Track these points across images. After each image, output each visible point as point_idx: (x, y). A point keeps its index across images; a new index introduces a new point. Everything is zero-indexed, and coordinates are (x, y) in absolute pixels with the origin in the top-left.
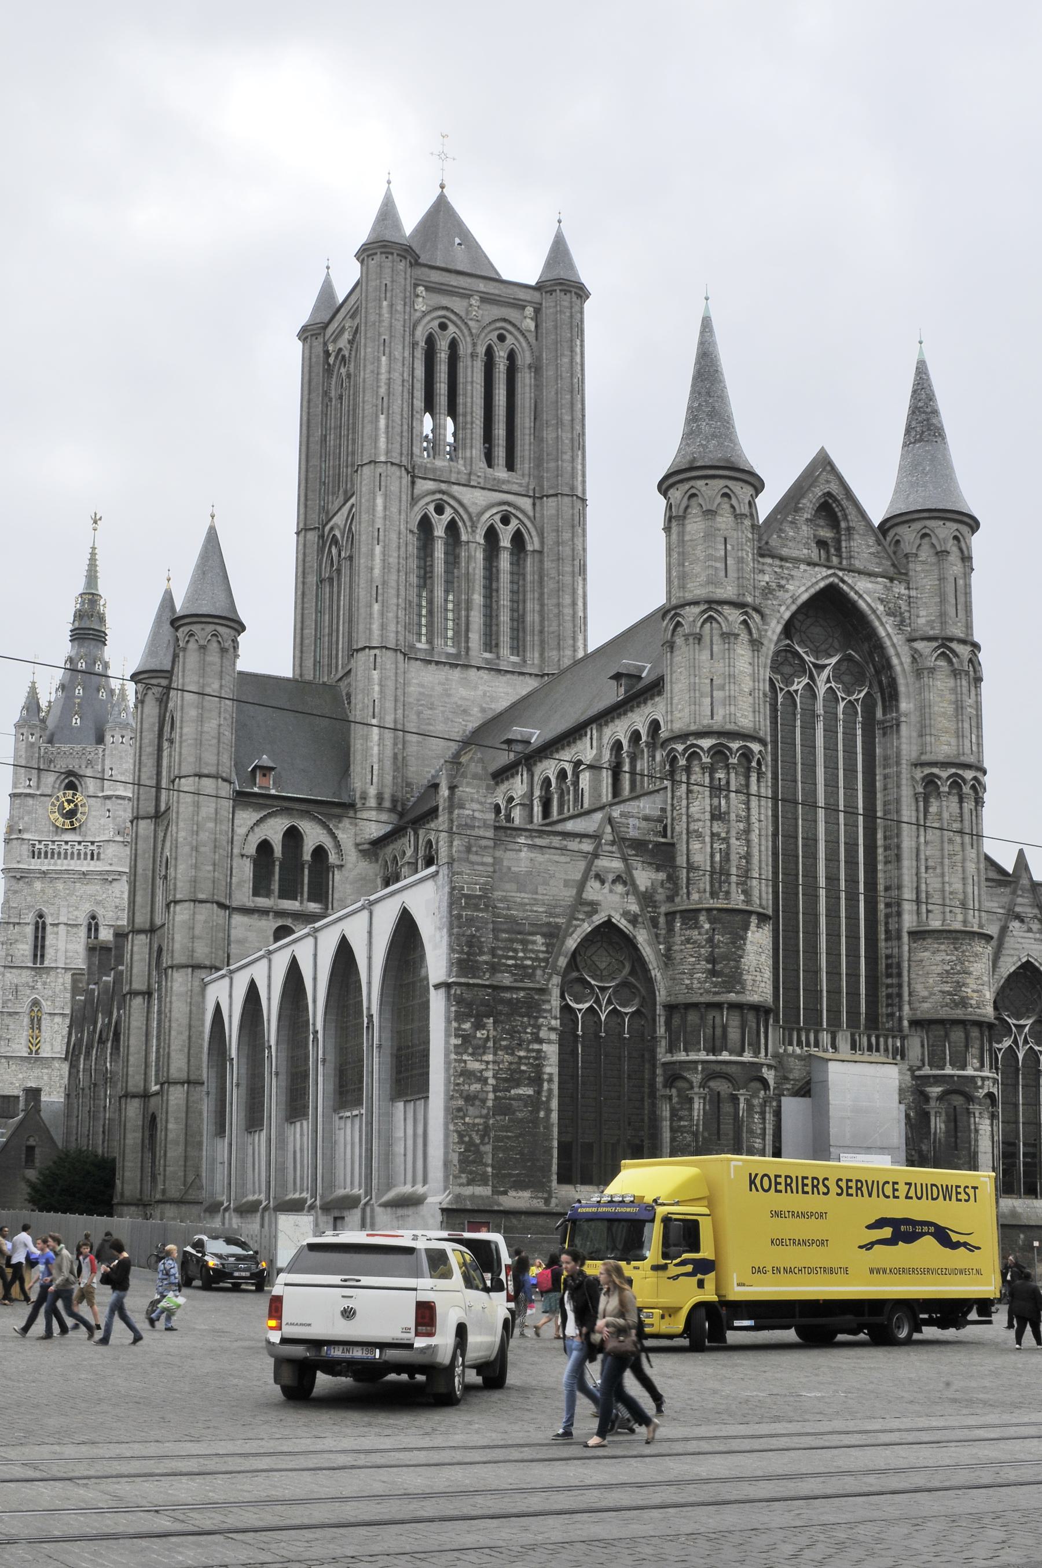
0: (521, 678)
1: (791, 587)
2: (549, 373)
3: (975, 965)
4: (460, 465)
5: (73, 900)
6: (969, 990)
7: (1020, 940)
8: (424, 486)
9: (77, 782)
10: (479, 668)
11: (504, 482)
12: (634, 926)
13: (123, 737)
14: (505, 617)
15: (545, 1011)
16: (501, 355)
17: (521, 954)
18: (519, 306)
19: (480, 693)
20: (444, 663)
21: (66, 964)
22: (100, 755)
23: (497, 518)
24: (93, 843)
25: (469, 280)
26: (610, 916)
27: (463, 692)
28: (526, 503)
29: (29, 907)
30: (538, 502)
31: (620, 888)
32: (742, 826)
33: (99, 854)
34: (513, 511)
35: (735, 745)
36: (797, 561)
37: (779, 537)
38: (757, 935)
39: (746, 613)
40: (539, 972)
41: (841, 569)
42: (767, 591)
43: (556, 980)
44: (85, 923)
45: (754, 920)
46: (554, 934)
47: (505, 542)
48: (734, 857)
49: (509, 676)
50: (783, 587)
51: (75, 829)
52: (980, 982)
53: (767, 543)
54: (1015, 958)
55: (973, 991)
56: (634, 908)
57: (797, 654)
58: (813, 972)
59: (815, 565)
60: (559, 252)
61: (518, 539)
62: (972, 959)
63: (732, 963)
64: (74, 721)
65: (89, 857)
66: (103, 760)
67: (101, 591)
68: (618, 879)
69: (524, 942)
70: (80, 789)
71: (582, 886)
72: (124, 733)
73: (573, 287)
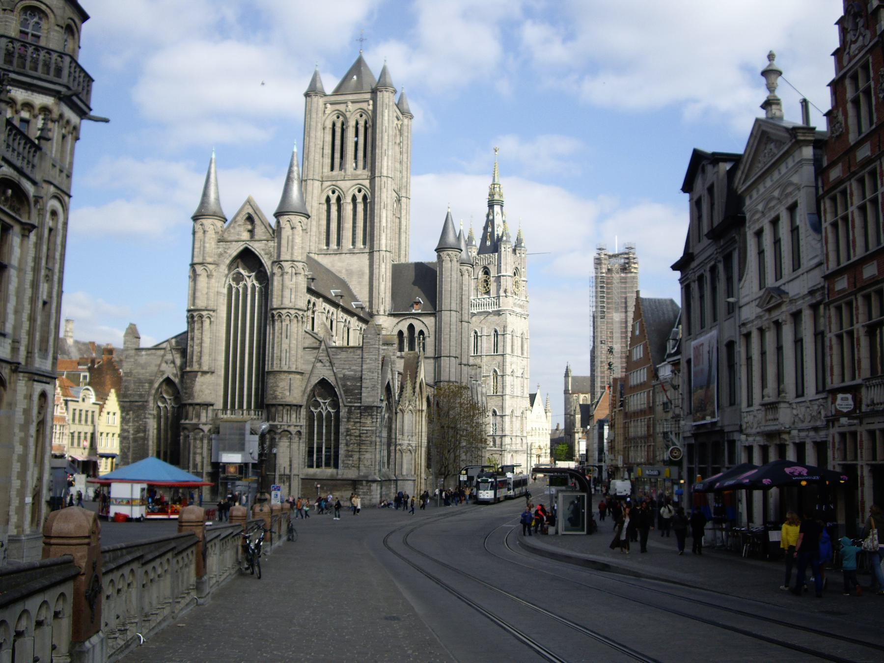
1: (229, 251)
4: (342, 172)
11: (360, 175)
16: (362, 123)
27: (339, 264)
28: (367, 183)
32: (199, 341)
35: (195, 314)
42: (220, 255)
43: (151, 398)
44: (493, 333)
45: (199, 374)
46: (151, 383)
47: (360, 199)
48: (195, 353)
56: (175, 372)
57: (241, 274)
60: (384, 72)
69: (143, 386)
71: (160, 366)
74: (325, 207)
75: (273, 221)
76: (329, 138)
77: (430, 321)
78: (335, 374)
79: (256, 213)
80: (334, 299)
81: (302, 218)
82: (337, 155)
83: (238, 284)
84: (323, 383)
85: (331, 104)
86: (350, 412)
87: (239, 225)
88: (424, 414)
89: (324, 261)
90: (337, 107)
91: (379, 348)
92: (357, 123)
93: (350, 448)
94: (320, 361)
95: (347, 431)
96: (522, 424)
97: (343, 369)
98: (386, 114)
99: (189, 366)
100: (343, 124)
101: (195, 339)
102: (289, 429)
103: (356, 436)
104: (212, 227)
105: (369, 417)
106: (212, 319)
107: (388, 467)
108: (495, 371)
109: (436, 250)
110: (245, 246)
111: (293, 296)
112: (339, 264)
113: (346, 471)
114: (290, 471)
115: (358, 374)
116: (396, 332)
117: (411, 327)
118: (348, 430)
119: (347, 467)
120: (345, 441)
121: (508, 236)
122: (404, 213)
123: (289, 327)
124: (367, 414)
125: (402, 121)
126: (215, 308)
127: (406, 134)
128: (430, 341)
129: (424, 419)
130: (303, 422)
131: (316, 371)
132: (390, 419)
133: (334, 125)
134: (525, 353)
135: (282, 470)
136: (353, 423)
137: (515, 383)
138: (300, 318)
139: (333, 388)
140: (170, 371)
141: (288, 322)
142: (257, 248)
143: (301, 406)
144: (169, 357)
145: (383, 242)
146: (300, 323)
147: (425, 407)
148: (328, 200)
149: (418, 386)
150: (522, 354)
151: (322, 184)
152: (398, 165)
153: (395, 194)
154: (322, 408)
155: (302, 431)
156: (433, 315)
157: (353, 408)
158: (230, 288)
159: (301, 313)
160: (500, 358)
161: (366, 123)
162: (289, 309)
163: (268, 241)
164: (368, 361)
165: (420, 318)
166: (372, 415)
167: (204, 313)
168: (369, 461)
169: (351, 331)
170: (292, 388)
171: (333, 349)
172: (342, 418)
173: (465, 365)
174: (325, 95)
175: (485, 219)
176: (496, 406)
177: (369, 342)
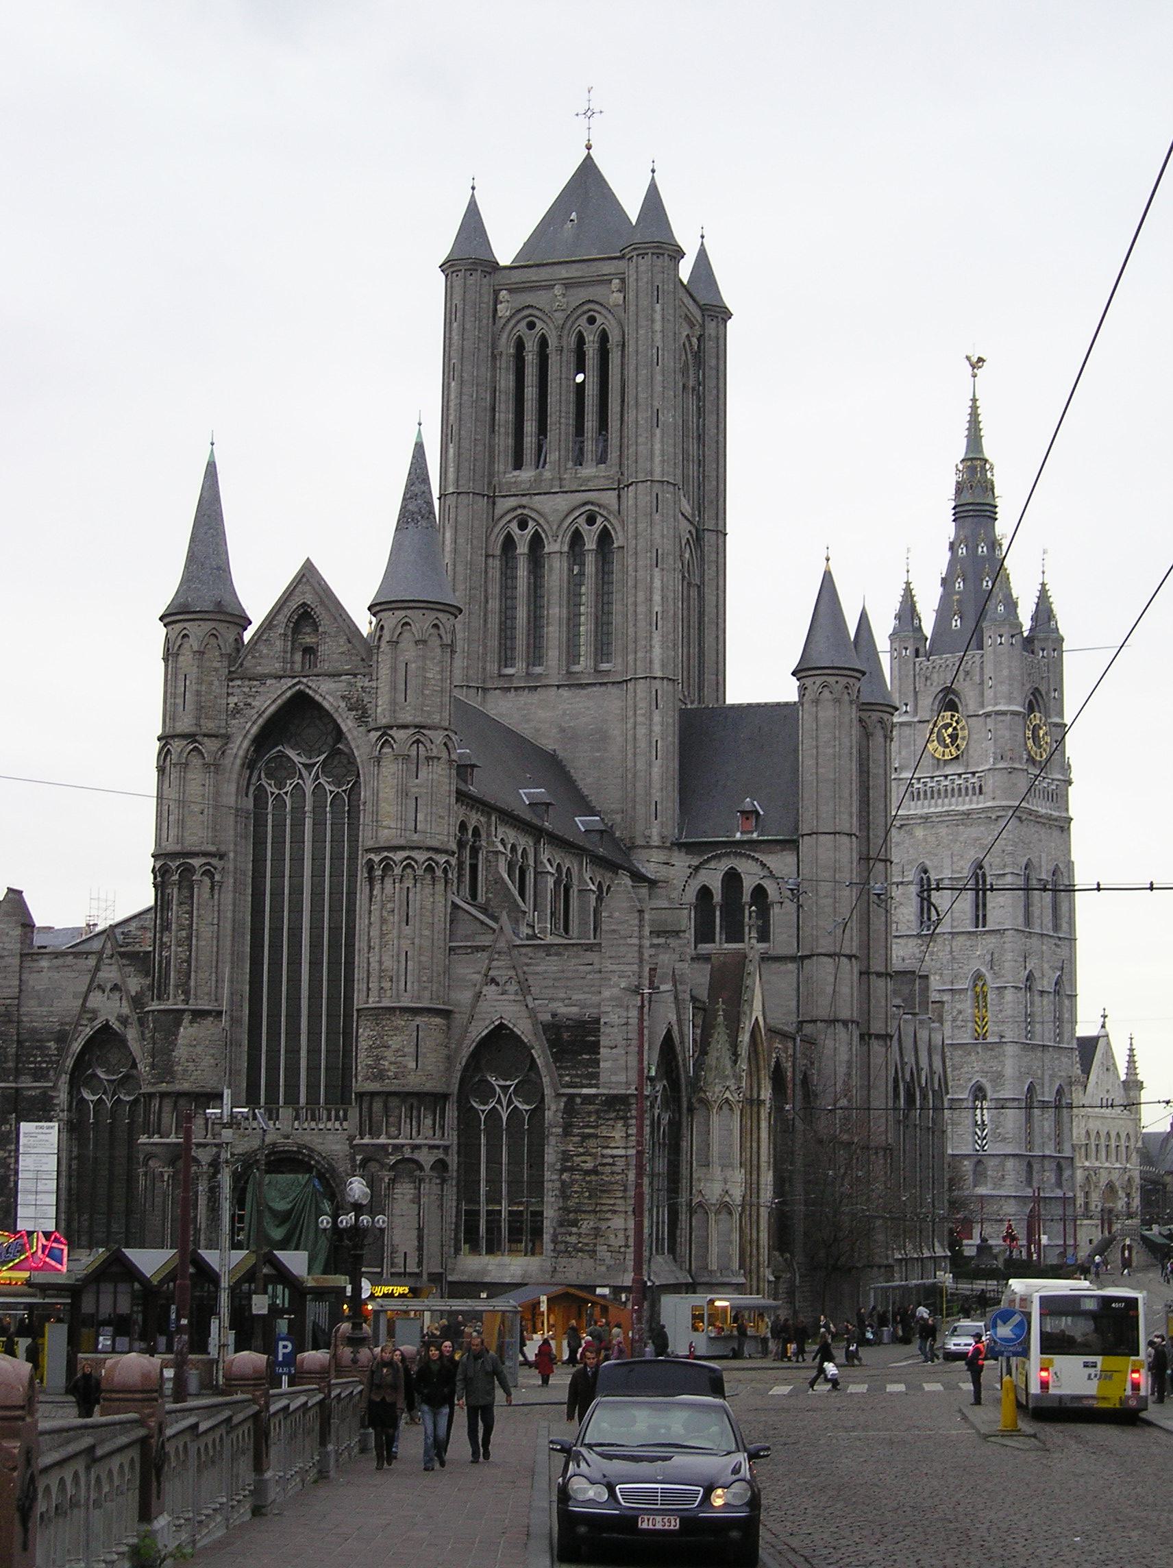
0: (603, 688)
2: (631, 348)
3: (395, 1038)
5: (956, 847)
6: (386, 1063)
7: (495, 1004)
8: (504, 504)
9: (956, 700)
10: (558, 687)
11: (588, 480)
12: (126, 1027)
13: (1001, 636)
14: (586, 627)
15: (56, 1105)
16: (591, 340)
17: (39, 1059)
18: (605, 281)
19: (561, 712)
20: (523, 688)
21: (952, 927)
22: (978, 663)
23: (582, 520)
24: (974, 773)
25: (548, 269)
26: (107, 1021)
27: (542, 714)
28: (610, 498)
29: (910, 862)
30: (624, 493)
31: (117, 995)
32: (184, 933)
33: (980, 787)
34: (597, 509)
35: (173, 865)
36: (262, 678)
37: (253, 657)
38: (190, 1030)
39: (196, 741)
40: (52, 1073)
41: (304, 677)
42: (236, 712)
43: (65, 1078)
45: (187, 1018)
46: (63, 1038)
47: (590, 544)
49: (590, 689)
50: (250, 705)
51: (957, 758)
52: (400, 1054)
53: (241, 665)
54: (487, 1022)
55: (391, 1063)
56: (126, 1010)
57: (288, 757)
58: (293, 1051)
59: (281, 677)
60: (653, 201)
61: (605, 537)
62: (390, 1033)
63: (165, 1057)
64: (954, 623)
65: (970, 792)
66: (982, 669)
67: (987, 454)
68: (115, 988)
70: (960, 709)
72: (1002, 631)
73: (648, 248)
74: (496, 563)
75: (364, 623)
76: (506, 381)
77: (781, 863)
78: (532, 1014)
79: (322, 602)
80: (528, 816)
81: (440, 615)
82: (530, 427)
83: (281, 785)
84: (500, 1036)
85: (510, 291)
86: (570, 1109)
87: (285, 635)
88: (764, 1114)
89: (502, 708)
90: (528, 298)
91: (641, 946)
92: (581, 340)
93: (570, 1203)
94: (493, 981)
95: (565, 1160)
96: (1058, 1123)
97: (552, 999)
98: (658, 317)
99: (159, 998)
100: (543, 342)
101: (174, 927)
102: (416, 1156)
103: (587, 1173)
104: (213, 641)
105: (620, 1124)
106: (217, 878)
107: (672, 1250)
108: (978, 976)
109: (794, 674)
110: (297, 687)
111: (420, 817)
112: (542, 714)
113: (563, 1261)
114: (420, 1264)
115: (590, 1012)
116: (691, 896)
117: (732, 879)
118: (566, 1156)
119: (564, 1251)
120: (558, 1184)
121: (1012, 605)
122: (710, 573)
123: (411, 895)
124: (613, 1115)
125: (703, 326)
126: (223, 849)
127: (713, 362)
128: (781, 916)
129: (764, 1124)
130: (452, 1139)
131: (483, 1006)
132: (675, 1126)
133: (520, 345)
134: (1065, 926)
135: (399, 1260)
136: (577, 1139)
137: (1037, 1009)
138: (439, 873)
139: (526, 1049)
140: (109, 1008)
141: (409, 883)
142: (327, 693)
143: (445, 1097)
144: (109, 974)
145: (657, 651)
146: (440, 887)
147: (766, 1094)
148: (509, 543)
149: (745, 1038)
150: (1056, 927)
151: (494, 503)
152: (693, 448)
153: (684, 523)
154: (499, 1102)
155: (448, 1159)
156: (791, 844)
157: (578, 1100)
158: (260, 797)
159: (442, 859)
160: (992, 940)
161: (604, 338)
162: (412, 848)
163: (355, 675)
164: (615, 979)
165: (757, 856)
166: (625, 1118)
167: (196, 862)
168: (621, 1235)
169: (574, 892)
170: (422, 1050)
171: (523, 950)
172: (551, 1126)
173: (879, 975)
174: (494, 266)
175: (948, 555)
176: (984, 1073)
177: (614, 931)
